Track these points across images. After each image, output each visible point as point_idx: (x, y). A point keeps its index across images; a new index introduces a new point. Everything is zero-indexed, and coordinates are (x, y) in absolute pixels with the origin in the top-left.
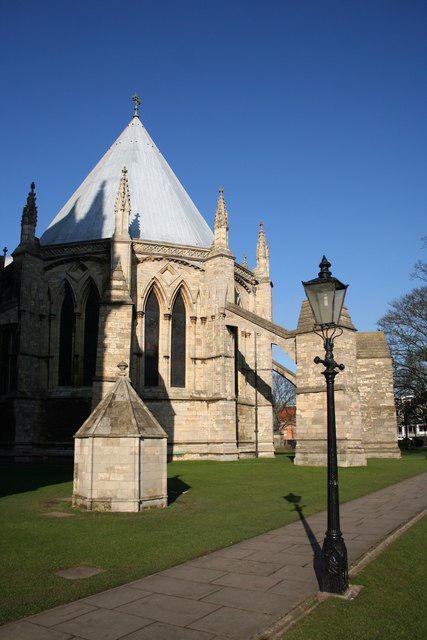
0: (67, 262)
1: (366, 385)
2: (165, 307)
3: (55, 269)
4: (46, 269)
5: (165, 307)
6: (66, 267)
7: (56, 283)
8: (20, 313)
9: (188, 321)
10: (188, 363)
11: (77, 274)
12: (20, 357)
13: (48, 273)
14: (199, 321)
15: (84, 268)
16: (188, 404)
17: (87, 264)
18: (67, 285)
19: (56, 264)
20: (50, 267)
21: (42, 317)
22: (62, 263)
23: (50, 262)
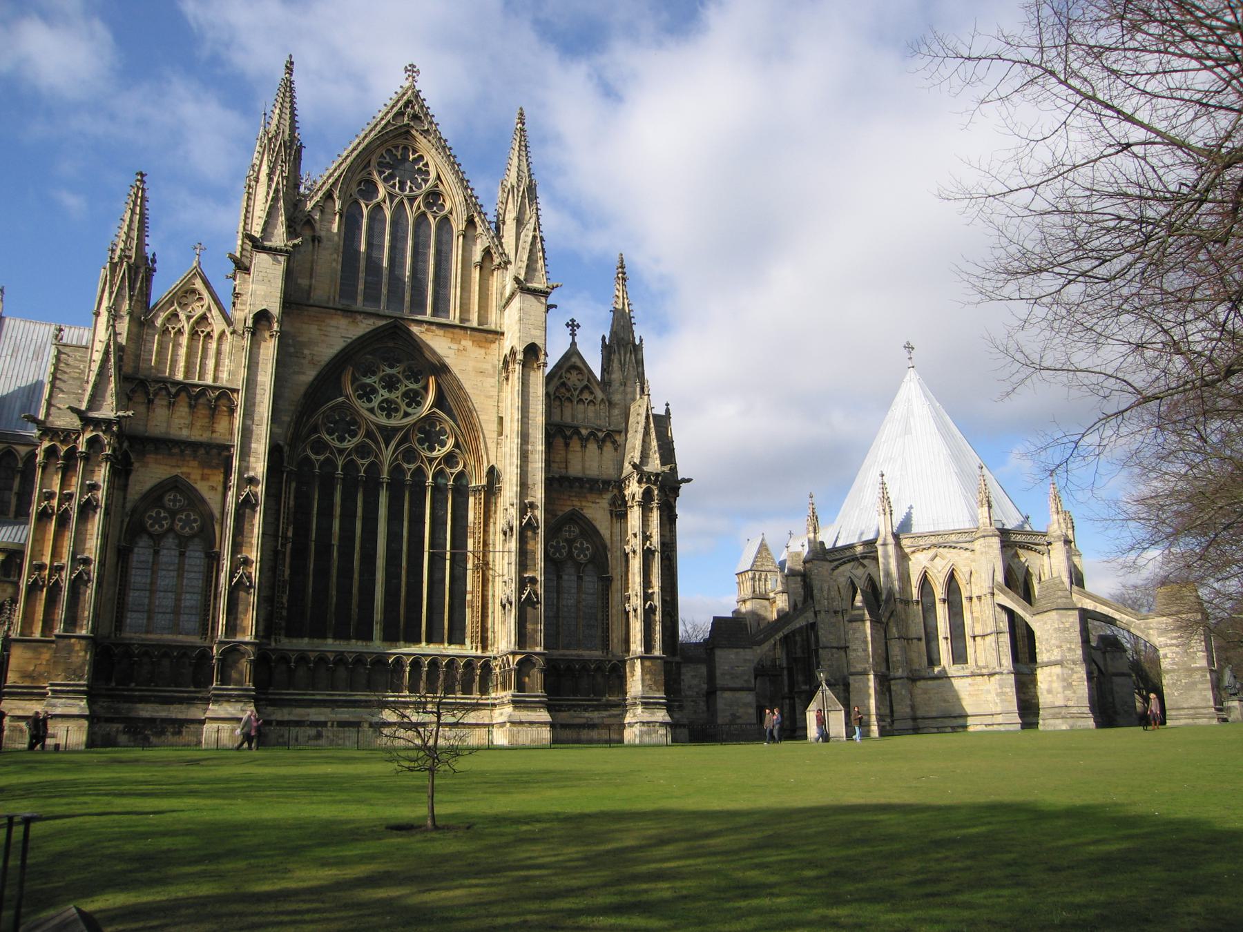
0: (849, 561)
1: (1172, 645)
2: (939, 592)
3: (841, 569)
4: (833, 570)
5: (939, 592)
6: (849, 566)
7: (843, 581)
8: (815, 613)
9: (965, 603)
10: (969, 641)
11: (860, 571)
12: (820, 650)
13: (836, 572)
14: (975, 600)
15: (864, 566)
16: (969, 680)
17: (866, 562)
18: (852, 583)
19: (841, 564)
20: (837, 567)
21: (836, 612)
22: (845, 563)
23: (836, 563)
